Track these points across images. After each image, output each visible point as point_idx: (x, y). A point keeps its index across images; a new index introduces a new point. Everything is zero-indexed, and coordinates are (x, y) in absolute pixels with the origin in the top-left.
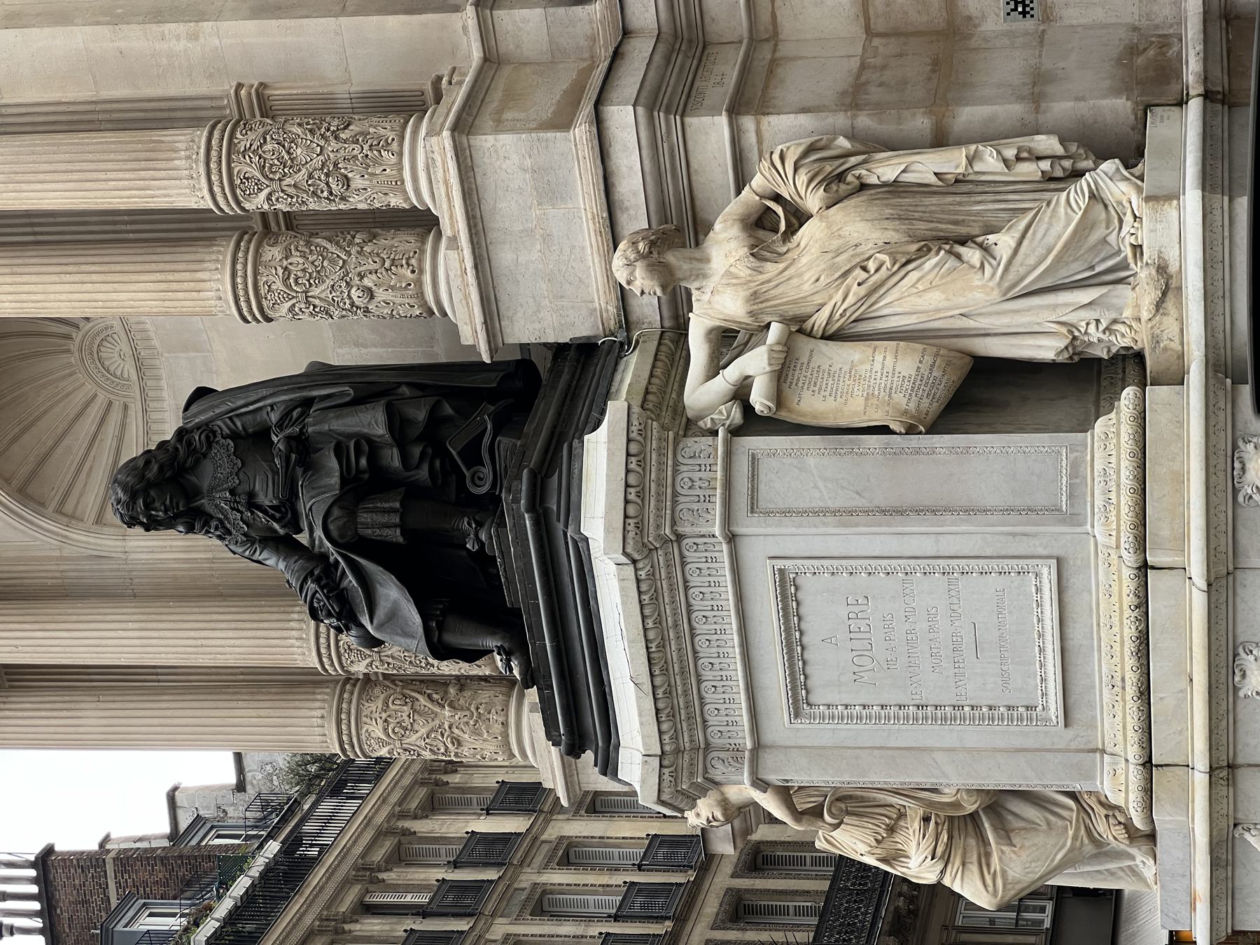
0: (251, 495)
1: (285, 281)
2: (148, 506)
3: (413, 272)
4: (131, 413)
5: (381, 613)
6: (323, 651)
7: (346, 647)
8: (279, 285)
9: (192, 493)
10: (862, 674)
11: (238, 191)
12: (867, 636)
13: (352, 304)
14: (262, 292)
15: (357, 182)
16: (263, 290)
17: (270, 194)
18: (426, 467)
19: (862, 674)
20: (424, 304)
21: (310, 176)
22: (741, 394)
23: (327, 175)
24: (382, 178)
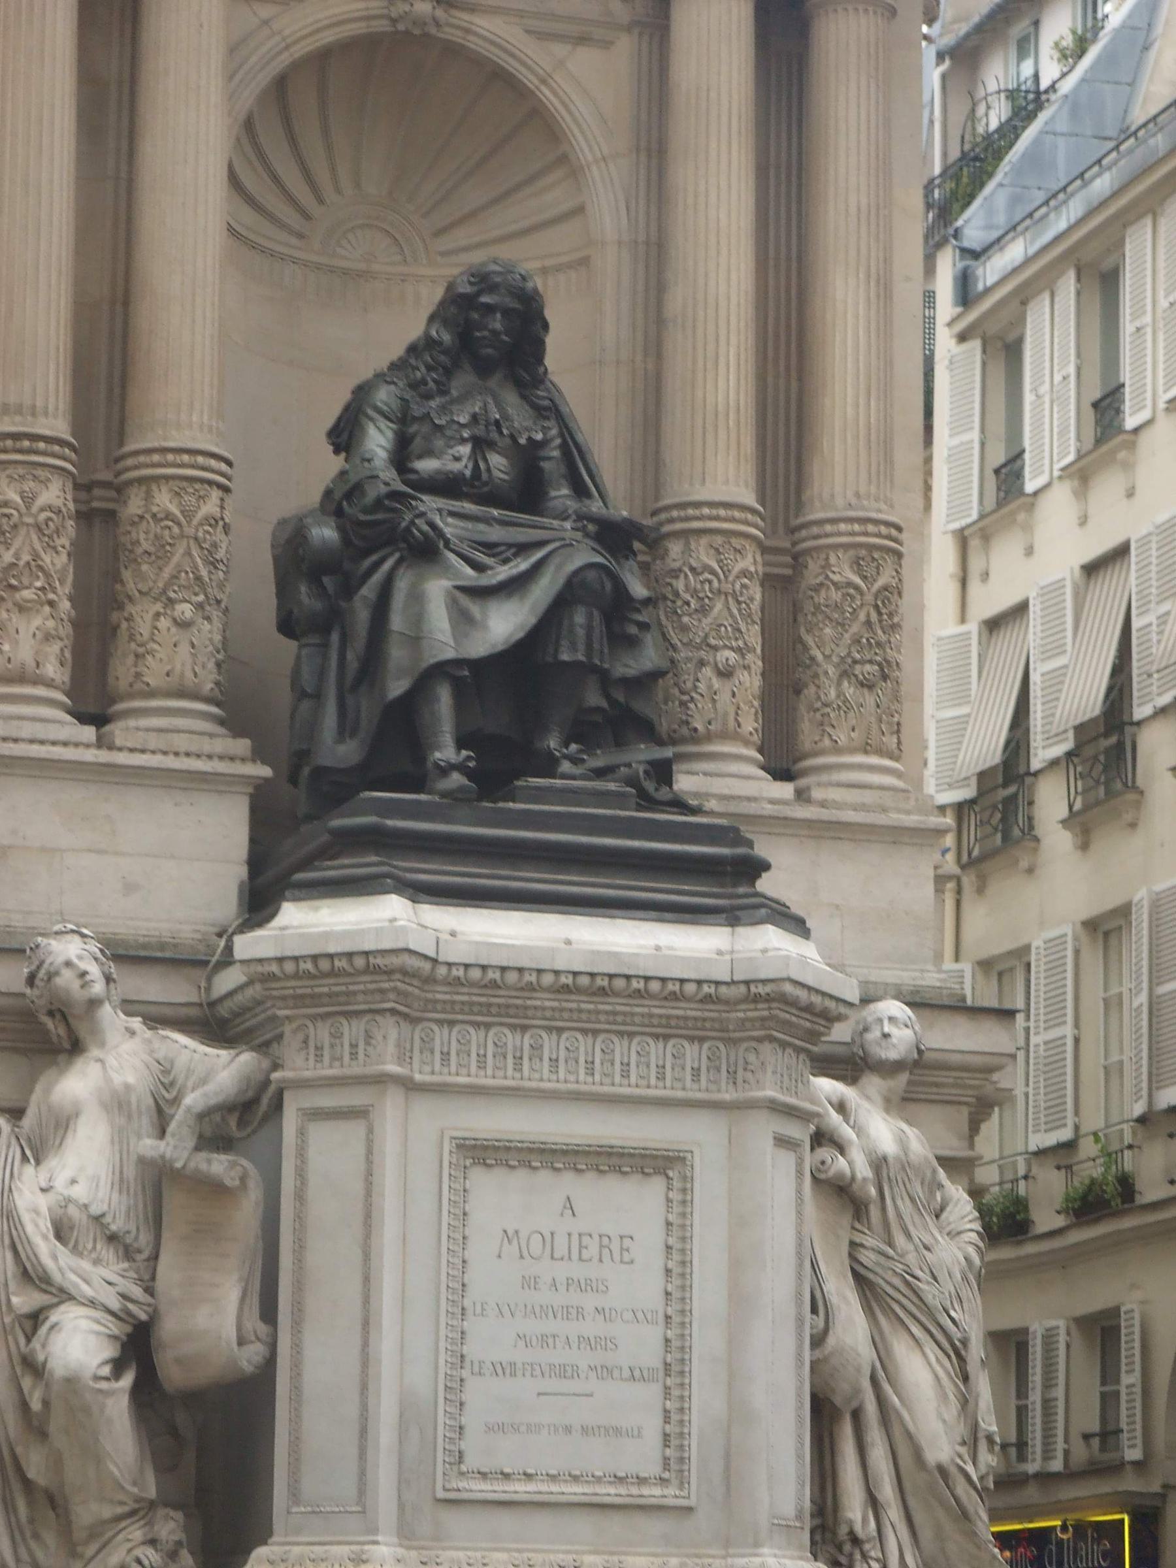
0: (491, 445)
1: (744, 573)
2: (507, 312)
3: (751, 733)
4: (294, 241)
5: (465, 601)
6: (200, 459)
7: (202, 493)
8: (741, 565)
9: (484, 369)
10: (515, 1242)
11: (863, 552)
12: (575, 1255)
13: (715, 648)
14: (733, 540)
15: (870, 699)
16: (736, 542)
17: (857, 588)
18: (604, 704)
19: (515, 1242)
20: (709, 737)
21: (879, 644)
22: (821, 1138)
23: (880, 664)
24: (875, 726)
